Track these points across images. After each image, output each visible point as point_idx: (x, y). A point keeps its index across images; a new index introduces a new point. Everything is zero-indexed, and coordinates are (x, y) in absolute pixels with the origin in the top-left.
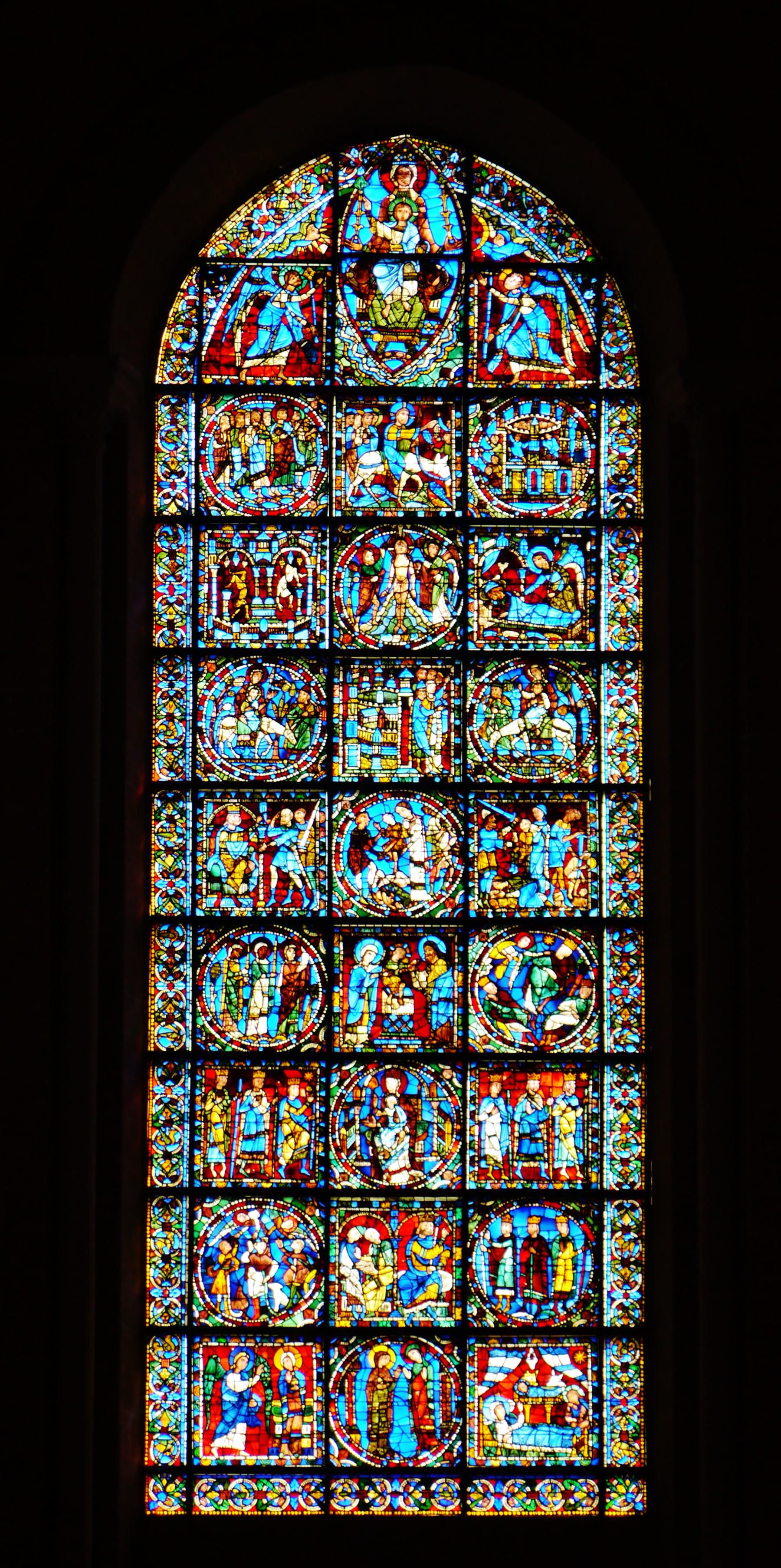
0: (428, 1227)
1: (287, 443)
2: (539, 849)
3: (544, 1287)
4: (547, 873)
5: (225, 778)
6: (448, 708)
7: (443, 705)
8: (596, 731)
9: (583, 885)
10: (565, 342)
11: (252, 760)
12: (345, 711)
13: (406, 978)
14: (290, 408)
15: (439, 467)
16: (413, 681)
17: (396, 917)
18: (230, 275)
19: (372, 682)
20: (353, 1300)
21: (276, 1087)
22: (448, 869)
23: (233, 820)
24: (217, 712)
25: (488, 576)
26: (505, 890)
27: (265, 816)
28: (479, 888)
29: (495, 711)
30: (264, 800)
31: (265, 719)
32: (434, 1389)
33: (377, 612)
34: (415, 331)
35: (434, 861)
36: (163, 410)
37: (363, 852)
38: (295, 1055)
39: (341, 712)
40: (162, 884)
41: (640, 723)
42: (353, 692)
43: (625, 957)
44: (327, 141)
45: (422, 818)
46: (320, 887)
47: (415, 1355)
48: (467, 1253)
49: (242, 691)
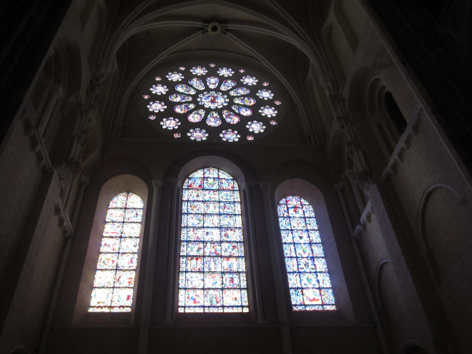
3: (233, 283)
17: (212, 241)
21: (197, 259)
32: (218, 296)
36: (184, 191)
38: (199, 256)
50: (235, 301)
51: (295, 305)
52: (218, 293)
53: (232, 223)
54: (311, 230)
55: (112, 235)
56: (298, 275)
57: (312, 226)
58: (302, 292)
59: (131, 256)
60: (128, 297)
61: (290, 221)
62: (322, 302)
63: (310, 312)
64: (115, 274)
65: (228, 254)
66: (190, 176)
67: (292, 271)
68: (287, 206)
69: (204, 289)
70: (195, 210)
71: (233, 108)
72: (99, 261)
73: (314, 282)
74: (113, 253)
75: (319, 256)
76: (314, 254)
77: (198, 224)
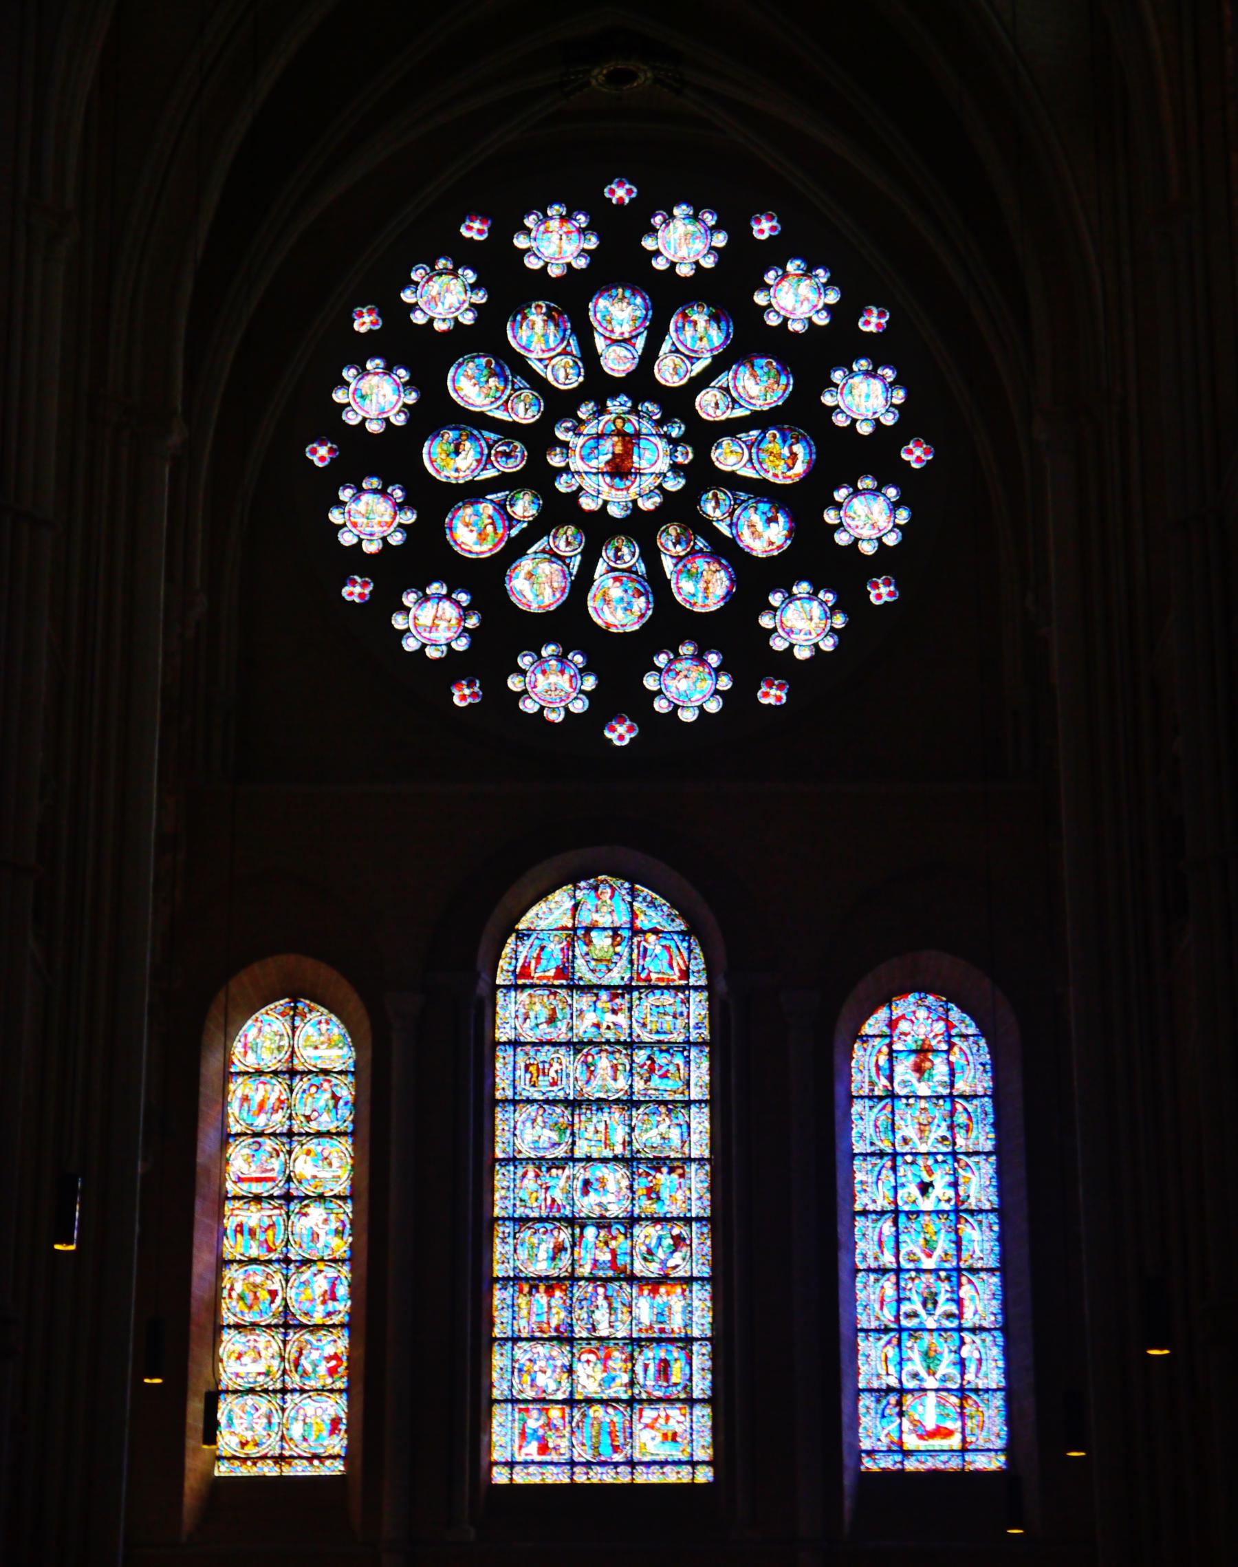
0: (616, 1354)
1: (554, 1010)
3: (667, 1379)
8: (689, 1135)
10: (675, 964)
13: (606, 1244)
14: (555, 994)
15: (621, 1019)
17: (602, 1217)
18: (529, 936)
20: (584, 1387)
21: (550, 1292)
23: (531, 1174)
25: (642, 1067)
33: (594, 1083)
34: (609, 961)
36: (500, 995)
38: (558, 1278)
42: (583, 1118)
43: (702, 1234)
44: (572, 879)
47: (610, 1410)
48: (634, 1365)
50: (672, 1444)
51: (870, 1453)
52: (615, 1416)
53: (675, 1140)
54: (967, 1154)
55: (257, 1188)
56: (895, 1341)
57: (973, 1135)
58: (899, 1403)
59: (331, 1273)
60: (335, 1422)
61: (893, 1112)
62: (964, 1440)
63: (916, 1474)
64: (285, 1342)
65: (653, 1270)
66: (520, 926)
67: (874, 1324)
68: (890, 1045)
69: (571, 1402)
70: (543, 1082)
71: (709, 508)
72: (225, 1293)
73: (945, 1367)
74: (270, 1262)
75: (979, 1265)
76: (965, 1255)
77: (554, 1145)
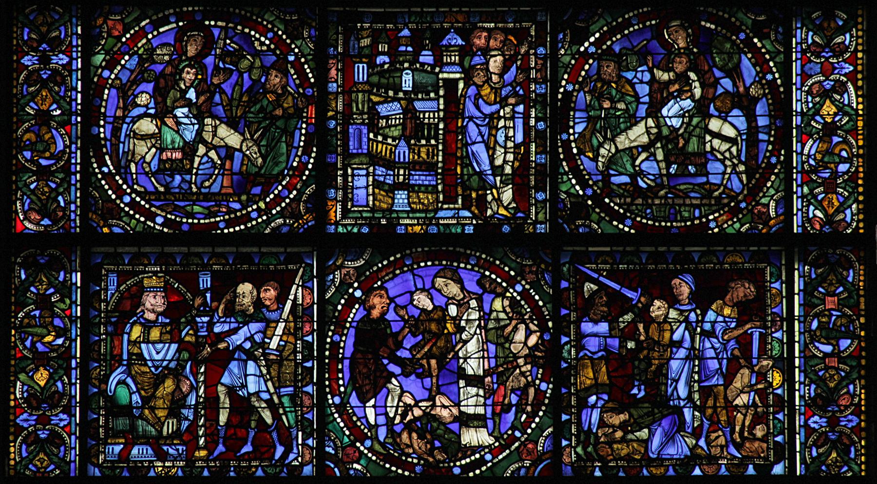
2: (682, 353)
4: (696, 396)
5: (139, 228)
6: (524, 100)
7: (515, 94)
8: (783, 140)
9: (758, 419)
11: (186, 195)
12: (347, 105)
16: (466, 51)
19: (393, 53)
22: (524, 391)
23: (153, 302)
24: (125, 109)
26: (623, 426)
27: (208, 295)
28: (579, 424)
29: (607, 105)
30: (205, 267)
31: (208, 121)
35: (500, 375)
37: (378, 359)
39: (340, 107)
40: (25, 420)
41: (860, 124)
42: (361, 71)
45: (480, 300)
46: (303, 424)
49: (169, 70)
